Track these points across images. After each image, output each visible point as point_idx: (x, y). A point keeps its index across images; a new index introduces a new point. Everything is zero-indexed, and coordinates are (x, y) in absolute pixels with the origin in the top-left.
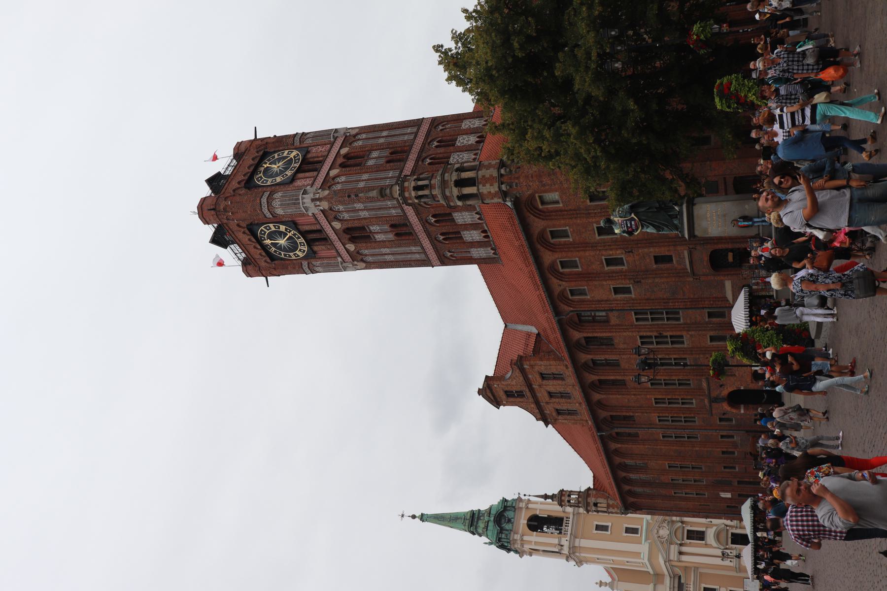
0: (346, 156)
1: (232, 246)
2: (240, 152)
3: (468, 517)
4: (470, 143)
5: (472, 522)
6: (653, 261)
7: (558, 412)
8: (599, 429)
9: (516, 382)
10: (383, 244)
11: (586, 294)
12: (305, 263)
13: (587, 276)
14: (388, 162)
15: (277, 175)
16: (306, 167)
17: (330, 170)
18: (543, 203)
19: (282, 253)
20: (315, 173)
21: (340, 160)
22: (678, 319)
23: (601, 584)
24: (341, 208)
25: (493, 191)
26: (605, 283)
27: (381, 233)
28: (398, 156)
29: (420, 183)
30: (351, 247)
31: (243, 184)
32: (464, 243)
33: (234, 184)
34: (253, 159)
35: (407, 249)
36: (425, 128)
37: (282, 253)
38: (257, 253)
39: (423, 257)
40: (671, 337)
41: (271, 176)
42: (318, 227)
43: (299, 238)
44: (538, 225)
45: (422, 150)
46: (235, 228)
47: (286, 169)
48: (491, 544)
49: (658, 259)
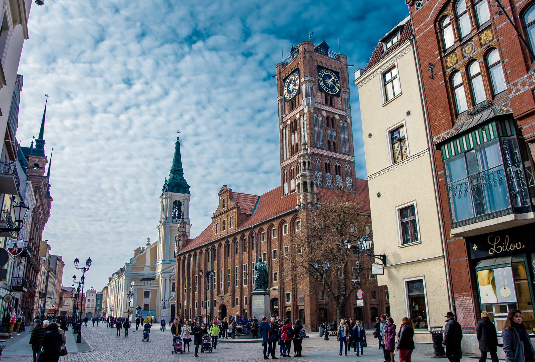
0: (333, 119)
5: (177, 169)
8: (210, 244)
14: (329, 141)
15: (324, 82)
16: (329, 97)
18: (298, 222)
20: (324, 103)
21: (331, 116)
23: (149, 239)
25: (301, 200)
27: (295, 139)
28: (332, 146)
30: (289, 123)
39: (285, 159)
41: (324, 79)
44: (288, 219)
47: (328, 87)
48: (166, 181)
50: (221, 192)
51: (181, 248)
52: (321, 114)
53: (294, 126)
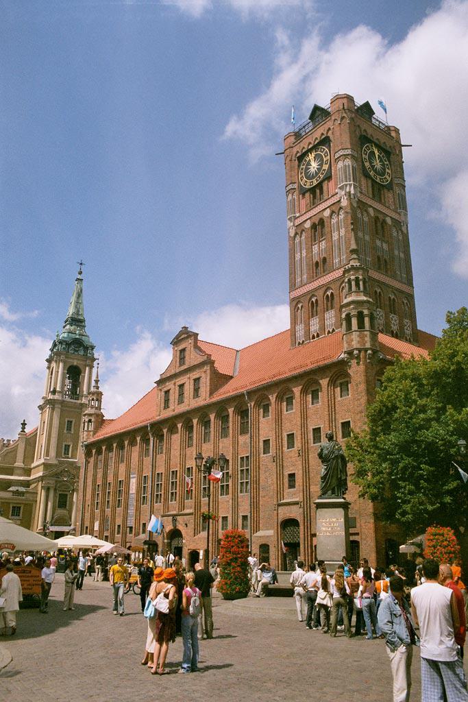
0: (384, 221)
1: (311, 124)
2: (391, 133)
3: (80, 317)
4: (392, 325)
6: (290, 473)
7: (167, 392)
8: (153, 425)
9: (193, 358)
10: (310, 250)
11: (264, 417)
12: (296, 186)
13: (279, 420)
15: (371, 163)
17: (374, 208)
19: (304, 167)
20: (371, 196)
21: (381, 216)
22: (241, 492)
24: (342, 217)
25: (353, 343)
26: (274, 432)
27: (319, 249)
29: (361, 283)
30: (308, 225)
31: (365, 134)
32: (309, 319)
33: (364, 126)
34: (385, 143)
35: (305, 271)
36: (404, 288)
37: (304, 167)
38: (305, 144)
40: (228, 485)
42: (325, 198)
43: (317, 180)
45: (388, 286)
46: (326, 126)
47: (375, 171)
49: (292, 476)
50: (177, 337)
51: (92, 433)
52: (366, 211)
53: (319, 227)
